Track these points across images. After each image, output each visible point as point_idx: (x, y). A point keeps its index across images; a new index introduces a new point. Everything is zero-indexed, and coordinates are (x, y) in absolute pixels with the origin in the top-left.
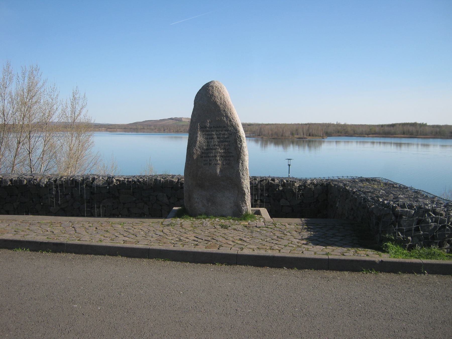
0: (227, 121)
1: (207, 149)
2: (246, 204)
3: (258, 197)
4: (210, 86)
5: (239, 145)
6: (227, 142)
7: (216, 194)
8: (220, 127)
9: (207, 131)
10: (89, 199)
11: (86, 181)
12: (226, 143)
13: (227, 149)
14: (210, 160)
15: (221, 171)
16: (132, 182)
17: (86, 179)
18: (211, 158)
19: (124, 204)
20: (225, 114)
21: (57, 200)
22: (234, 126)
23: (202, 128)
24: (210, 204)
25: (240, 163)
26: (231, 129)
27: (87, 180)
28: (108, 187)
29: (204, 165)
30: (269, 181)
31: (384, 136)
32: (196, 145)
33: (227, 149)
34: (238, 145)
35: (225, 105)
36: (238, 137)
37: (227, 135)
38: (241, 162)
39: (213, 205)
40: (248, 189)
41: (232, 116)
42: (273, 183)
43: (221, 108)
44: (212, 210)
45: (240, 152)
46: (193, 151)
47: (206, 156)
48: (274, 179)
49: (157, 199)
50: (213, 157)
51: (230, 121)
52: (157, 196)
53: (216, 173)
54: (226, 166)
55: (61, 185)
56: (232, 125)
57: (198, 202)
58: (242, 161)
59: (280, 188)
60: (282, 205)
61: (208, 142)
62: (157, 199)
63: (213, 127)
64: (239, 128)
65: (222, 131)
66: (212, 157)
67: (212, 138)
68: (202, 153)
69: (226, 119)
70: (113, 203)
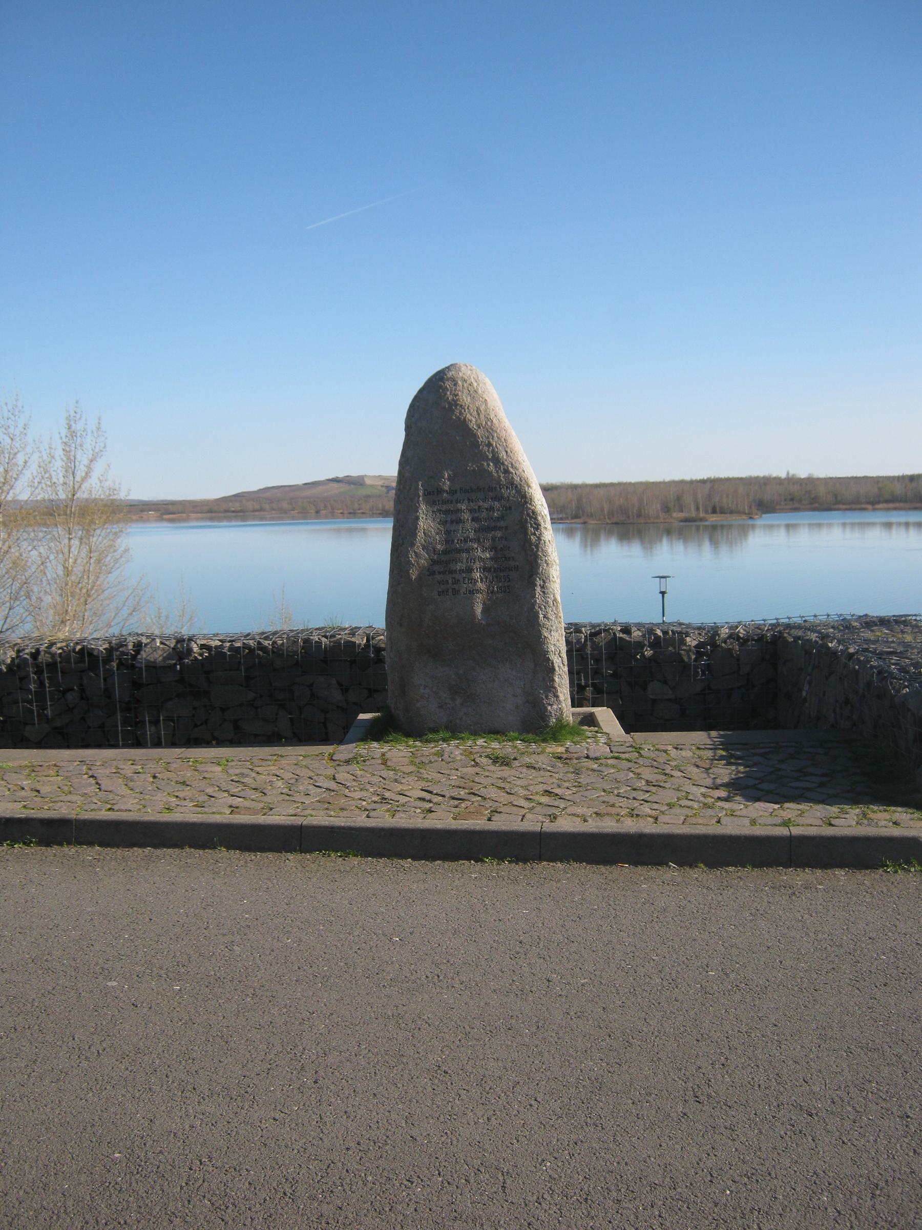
0: (497, 472)
1: (445, 552)
2: (557, 697)
3: (586, 678)
4: (448, 379)
5: (532, 537)
6: (500, 529)
8: (479, 489)
9: (445, 502)
10: (127, 699)
11: (118, 653)
12: (499, 534)
13: (501, 549)
14: (456, 582)
15: (486, 610)
16: (244, 651)
17: (119, 648)
18: (457, 576)
19: (223, 710)
20: (492, 454)
21: (43, 707)
22: (516, 487)
23: (429, 493)
24: (458, 701)
25: (536, 585)
26: (509, 494)
27: (121, 649)
28: (178, 667)
29: (439, 595)
30: (614, 634)
32: (415, 540)
33: (499, 548)
34: (530, 538)
35: (490, 430)
36: (528, 515)
37: (498, 510)
38: (539, 582)
40: (562, 655)
41: (511, 458)
42: (627, 639)
43: (479, 438)
45: (536, 557)
46: (409, 558)
47: (442, 570)
48: (629, 628)
49: (313, 695)
50: (463, 572)
51: (506, 471)
52: (312, 685)
53: (473, 616)
54: (500, 596)
55: (52, 666)
56: (512, 484)
57: (427, 696)
58: (544, 582)
59: (646, 653)
60: (652, 697)
61: (448, 532)
62: (313, 695)
63: (461, 489)
64: (530, 491)
65: (484, 500)
66: (461, 571)
67: (459, 521)
68: (434, 562)
69: (496, 467)
70: (195, 708)
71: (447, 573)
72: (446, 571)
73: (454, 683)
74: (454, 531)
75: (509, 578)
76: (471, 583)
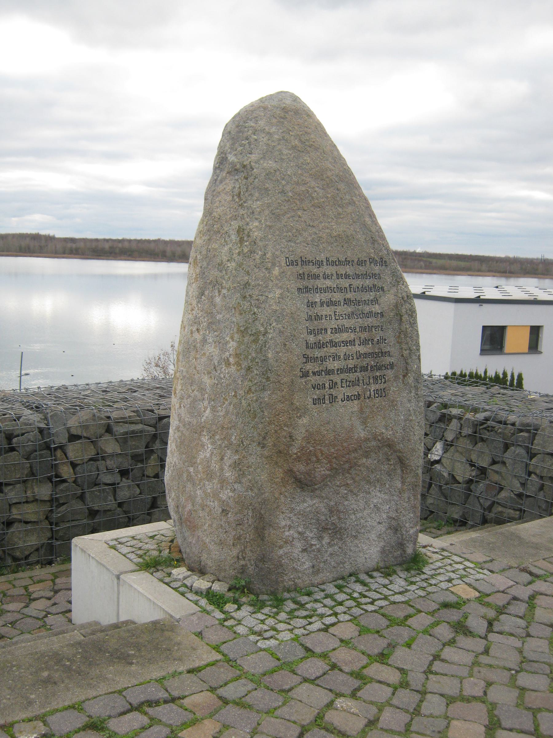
8: (347, 262)
14: (333, 385)
23: (292, 263)
24: (326, 540)
29: (314, 404)
31: (15, 253)
33: (376, 340)
47: (316, 370)
50: (341, 373)
71: (323, 373)
72: (322, 370)
73: (323, 518)
74: (326, 316)
76: (349, 386)
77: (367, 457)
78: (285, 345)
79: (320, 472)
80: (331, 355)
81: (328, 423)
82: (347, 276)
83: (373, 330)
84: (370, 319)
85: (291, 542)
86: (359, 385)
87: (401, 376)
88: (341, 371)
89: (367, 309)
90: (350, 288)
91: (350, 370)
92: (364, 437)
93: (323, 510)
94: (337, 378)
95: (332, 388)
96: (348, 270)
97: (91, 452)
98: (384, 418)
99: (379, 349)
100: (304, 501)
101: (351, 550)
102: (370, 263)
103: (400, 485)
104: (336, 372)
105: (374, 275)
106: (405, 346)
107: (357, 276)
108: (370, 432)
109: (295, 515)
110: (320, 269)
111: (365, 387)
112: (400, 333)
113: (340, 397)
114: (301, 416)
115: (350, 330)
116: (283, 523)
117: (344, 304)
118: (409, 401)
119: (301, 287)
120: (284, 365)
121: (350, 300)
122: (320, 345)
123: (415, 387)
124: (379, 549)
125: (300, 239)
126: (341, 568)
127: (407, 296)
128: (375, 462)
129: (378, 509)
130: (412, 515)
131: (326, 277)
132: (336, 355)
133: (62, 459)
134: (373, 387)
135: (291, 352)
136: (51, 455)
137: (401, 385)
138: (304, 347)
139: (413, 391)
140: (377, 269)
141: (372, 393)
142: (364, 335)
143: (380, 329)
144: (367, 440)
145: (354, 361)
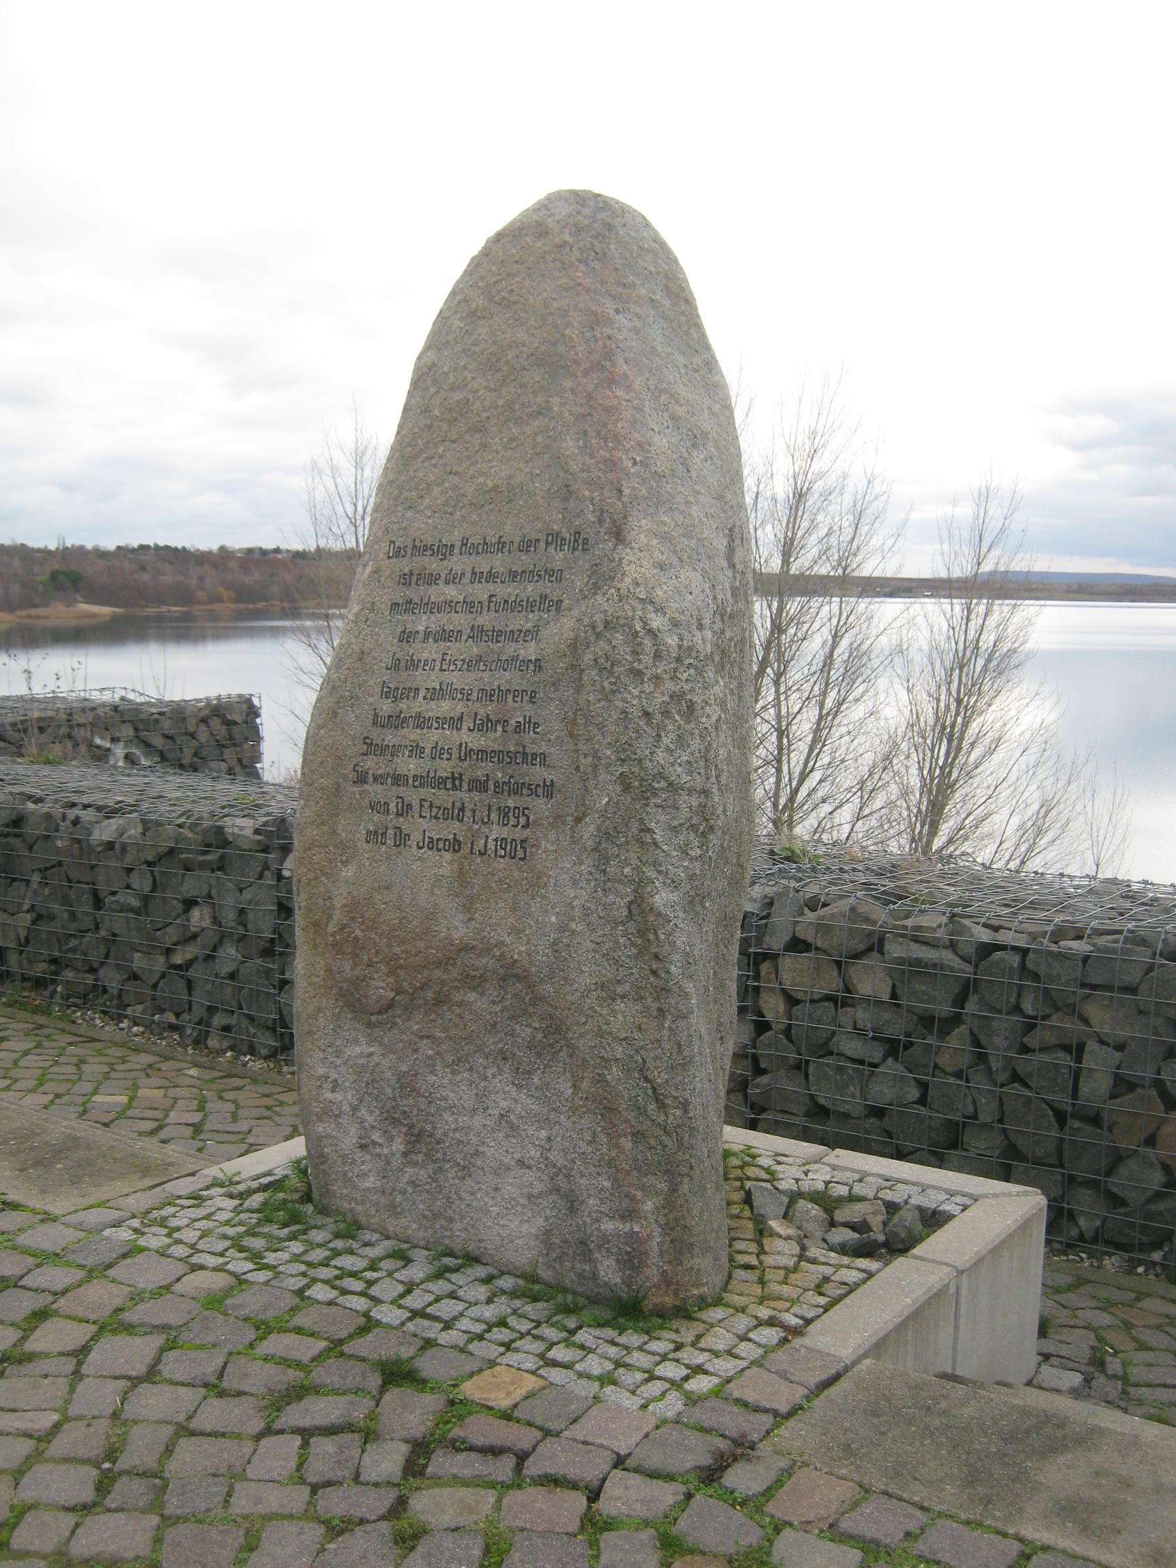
7: (432, 1079)
8: (501, 545)
13: (518, 728)
14: (405, 809)
23: (399, 553)
24: (398, 1145)
29: (368, 842)
33: (513, 722)
39: (420, 1157)
44: (410, 1190)
47: (380, 772)
50: (422, 785)
75: (528, 818)
76: (436, 818)
77: (474, 989)
78: (335, 714)
79: (378, 988)
80: (408, 743)
81: (388, 888)
82: (491, 577)
83: (510, 698)
84: (507, 674)
85: (336, 1116)
86: (461, 821)
87: (569, 819)
88: (422, 781)
89: (510, 649)
90: (490, 602)
91: (441, 783)
92: (461, 939)
93: (388, 1074)
94: (412, 796)
95: (402, 815)
96: (499, 563)
97: (831, 983)
98: (514, 910)
99: (517, 744)
100: (356, 1041)
101: (460, 1198)
102: (547, 544)
103: (570, 1091)
104: (410, 782)
105: (550, 572)
106: (582, 747)
107: (513, 576)
108: (479, 933)
109: (345, 1064)
110: (445, 562)
111: (476, 827)
112: (575, 714)
113: (416, 837)
114: (347, 861)
115: (460, 696)
116: (321, 1071)
117: (469, 637)
118: (575, 883)
119: (401, 601)
120: (324, 753)
121: (481, 630)
122: (396, 721)
123: (595, 849)
124: (533, 1231)
125: (427, 501)
126: (442, 1227)
127: (607, 624)
128: (497, 1008)
129: (513, 1127)
130: (607, 1184)
131: (452, 579)
132: (417, 746)
133: (769, 981)
134: (496, 832)
135: (343, 729)
136: (749, 965)
137: (565, 840)
138: (369, 723)
139: (589, 862)
140: (558, 558)
141: (491, 845)
142: (486, 709)
143: (526, 698)
144: (465, 948)
145: (451, 763)
